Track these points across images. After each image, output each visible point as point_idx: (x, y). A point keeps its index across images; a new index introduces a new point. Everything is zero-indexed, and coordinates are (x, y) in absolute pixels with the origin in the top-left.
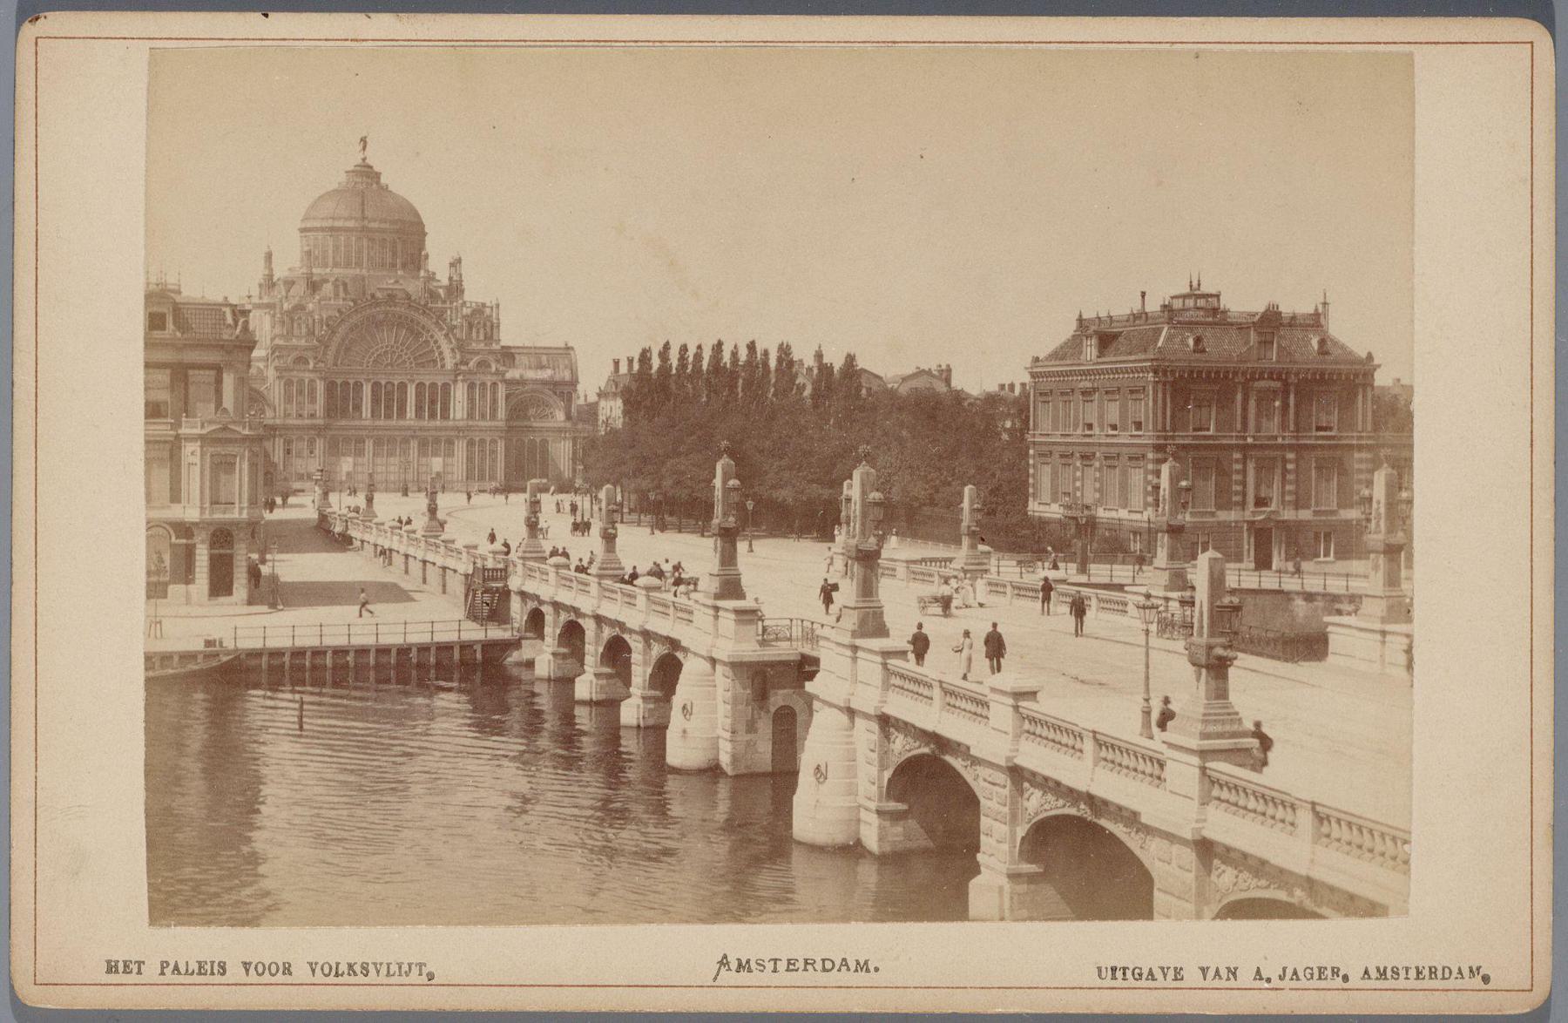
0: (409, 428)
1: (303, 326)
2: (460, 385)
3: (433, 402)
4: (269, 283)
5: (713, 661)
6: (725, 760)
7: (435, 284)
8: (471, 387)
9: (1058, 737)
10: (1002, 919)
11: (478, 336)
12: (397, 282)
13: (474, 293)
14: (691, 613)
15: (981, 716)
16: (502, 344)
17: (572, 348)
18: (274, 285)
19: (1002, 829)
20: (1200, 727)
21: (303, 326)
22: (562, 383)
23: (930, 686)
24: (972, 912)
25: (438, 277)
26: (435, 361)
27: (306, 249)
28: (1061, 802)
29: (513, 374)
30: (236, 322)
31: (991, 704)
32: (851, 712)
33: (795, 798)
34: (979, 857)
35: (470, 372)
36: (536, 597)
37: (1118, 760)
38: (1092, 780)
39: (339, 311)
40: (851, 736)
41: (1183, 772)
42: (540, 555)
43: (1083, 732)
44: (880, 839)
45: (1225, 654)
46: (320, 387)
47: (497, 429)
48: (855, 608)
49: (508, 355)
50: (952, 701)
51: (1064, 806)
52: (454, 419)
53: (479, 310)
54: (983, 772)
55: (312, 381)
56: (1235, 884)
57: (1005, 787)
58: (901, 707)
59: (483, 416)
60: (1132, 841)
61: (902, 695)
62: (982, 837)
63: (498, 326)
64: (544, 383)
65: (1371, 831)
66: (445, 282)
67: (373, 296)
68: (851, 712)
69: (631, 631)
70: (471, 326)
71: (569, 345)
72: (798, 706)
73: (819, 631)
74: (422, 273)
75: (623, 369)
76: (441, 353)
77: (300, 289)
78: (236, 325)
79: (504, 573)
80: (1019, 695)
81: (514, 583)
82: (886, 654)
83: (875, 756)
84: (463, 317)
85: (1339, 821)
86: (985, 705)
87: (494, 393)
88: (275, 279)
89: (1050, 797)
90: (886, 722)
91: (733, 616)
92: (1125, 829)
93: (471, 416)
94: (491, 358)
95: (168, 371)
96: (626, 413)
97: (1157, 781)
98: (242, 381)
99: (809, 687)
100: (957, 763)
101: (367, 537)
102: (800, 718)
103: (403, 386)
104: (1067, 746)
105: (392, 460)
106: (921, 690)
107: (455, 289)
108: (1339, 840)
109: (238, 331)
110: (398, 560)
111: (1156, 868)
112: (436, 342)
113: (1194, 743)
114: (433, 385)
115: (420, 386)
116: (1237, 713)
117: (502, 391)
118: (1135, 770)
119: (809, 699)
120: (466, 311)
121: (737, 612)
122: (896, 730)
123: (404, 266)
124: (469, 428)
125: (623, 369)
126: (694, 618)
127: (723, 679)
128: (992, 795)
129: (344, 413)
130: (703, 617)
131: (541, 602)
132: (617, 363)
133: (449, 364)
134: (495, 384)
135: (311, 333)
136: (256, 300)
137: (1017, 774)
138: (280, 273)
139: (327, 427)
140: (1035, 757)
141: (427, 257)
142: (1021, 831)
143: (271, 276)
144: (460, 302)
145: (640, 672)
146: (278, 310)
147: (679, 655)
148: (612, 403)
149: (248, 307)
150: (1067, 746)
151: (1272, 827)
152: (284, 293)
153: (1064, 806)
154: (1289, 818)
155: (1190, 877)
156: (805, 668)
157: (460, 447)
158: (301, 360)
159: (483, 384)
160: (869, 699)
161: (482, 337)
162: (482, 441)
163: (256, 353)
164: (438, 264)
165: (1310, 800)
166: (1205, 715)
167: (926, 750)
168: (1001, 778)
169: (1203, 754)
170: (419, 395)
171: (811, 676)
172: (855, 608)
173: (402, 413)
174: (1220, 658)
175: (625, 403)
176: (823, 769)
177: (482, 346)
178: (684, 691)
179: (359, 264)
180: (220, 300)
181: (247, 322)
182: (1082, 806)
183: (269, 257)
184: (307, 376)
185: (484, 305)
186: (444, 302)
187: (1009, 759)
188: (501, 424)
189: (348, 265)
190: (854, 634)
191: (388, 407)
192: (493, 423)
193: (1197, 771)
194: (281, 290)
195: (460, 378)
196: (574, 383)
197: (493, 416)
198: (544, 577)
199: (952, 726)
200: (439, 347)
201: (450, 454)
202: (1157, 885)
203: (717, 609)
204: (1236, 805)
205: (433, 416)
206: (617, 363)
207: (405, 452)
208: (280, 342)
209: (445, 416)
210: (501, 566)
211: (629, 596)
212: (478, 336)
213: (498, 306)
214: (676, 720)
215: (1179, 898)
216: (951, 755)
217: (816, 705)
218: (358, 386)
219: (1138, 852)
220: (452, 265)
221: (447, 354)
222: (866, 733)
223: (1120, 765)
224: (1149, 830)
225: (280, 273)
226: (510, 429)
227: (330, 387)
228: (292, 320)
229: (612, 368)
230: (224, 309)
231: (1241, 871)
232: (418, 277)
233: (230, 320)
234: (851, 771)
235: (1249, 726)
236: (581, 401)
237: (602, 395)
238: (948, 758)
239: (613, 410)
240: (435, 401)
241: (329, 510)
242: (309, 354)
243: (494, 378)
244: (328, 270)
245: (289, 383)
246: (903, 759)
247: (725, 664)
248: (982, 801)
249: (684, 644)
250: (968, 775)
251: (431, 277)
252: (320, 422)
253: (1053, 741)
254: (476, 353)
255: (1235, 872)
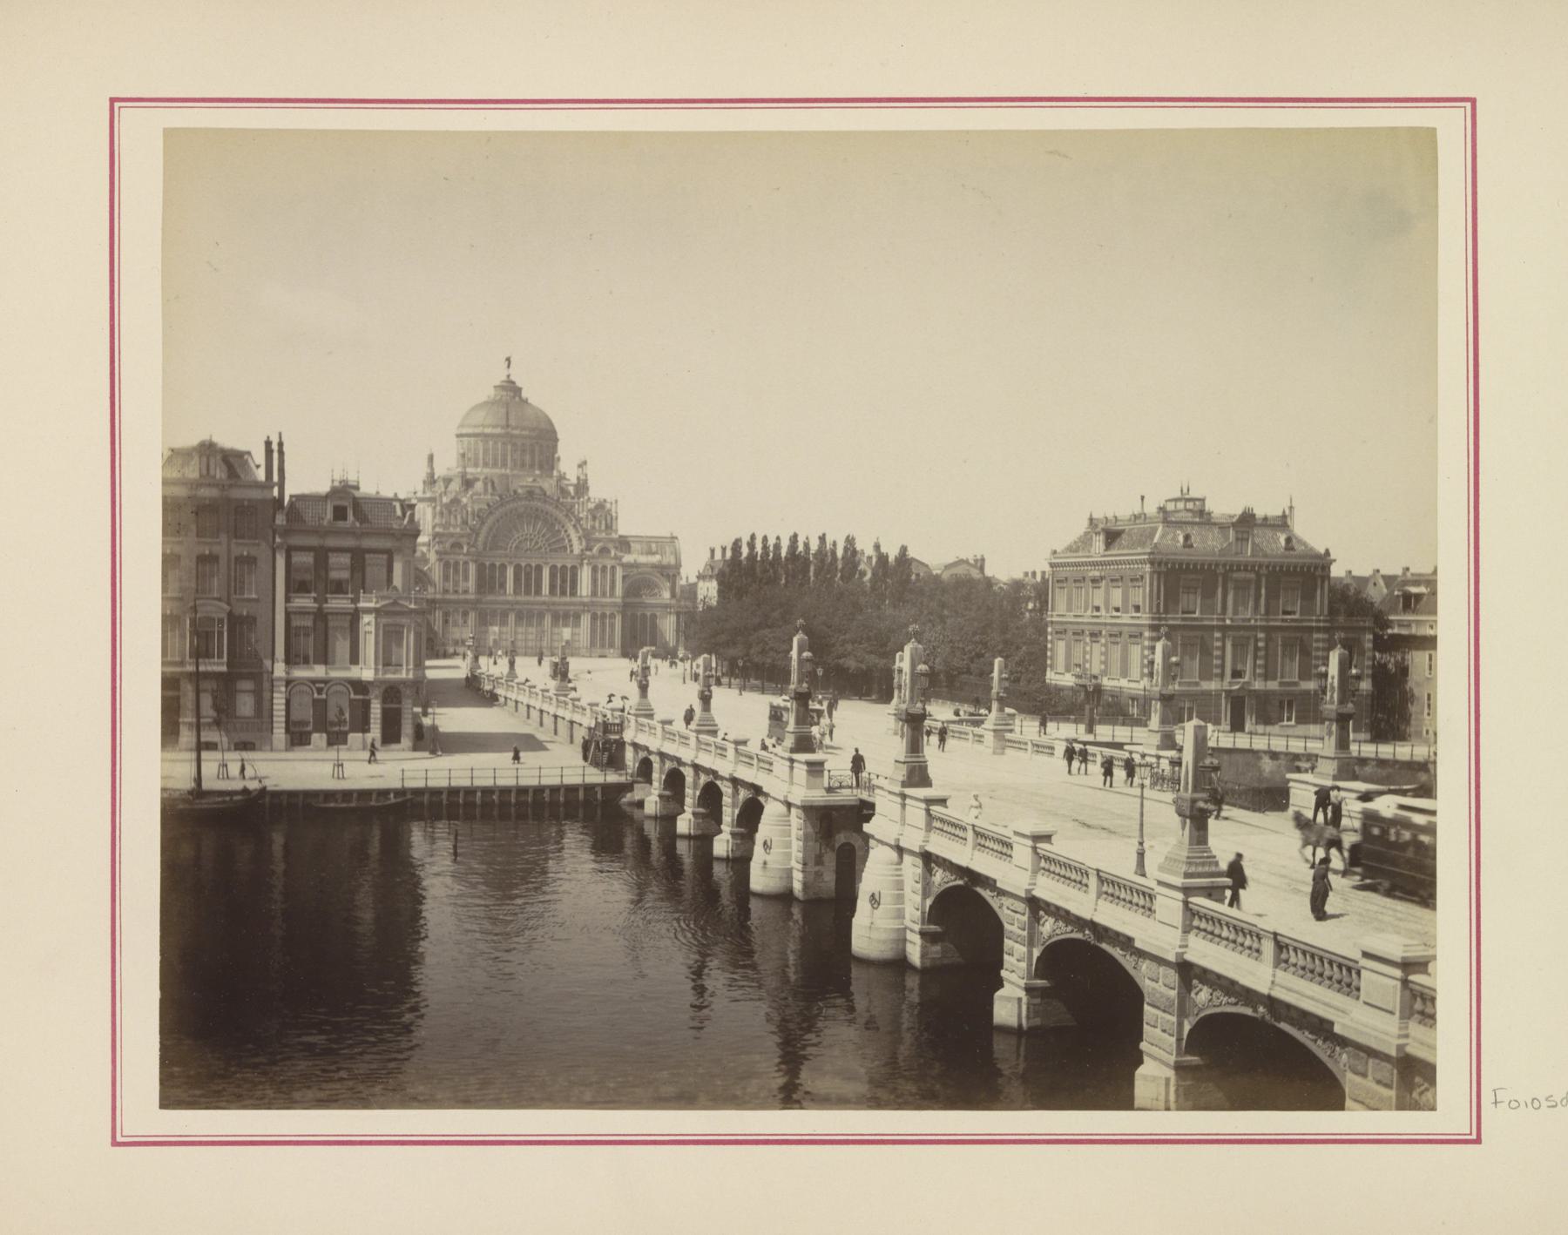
0: (544, 603)
1: (459, 517)
2: (585, 567)
3: (564, 581)
4: (431, 481)
5: (789, 805)
6: (797, 886)
7: (566, 482)
8: (594, 570)
9: (1068, 874)
10: (1168, 1109)
11: (600, 527)
12: (534, 480)
13: (596, 493)
14: (771, 764)
15: (1006, 854)
16: (622, 531)
17: (676, 538)
18: (435, 482)
19: (1021, 950)
20: (1184, 868)
21: (459, 517)
22: (668, 567)
23: (965, 829)
24: (1137, 1103)
25: (568, 477)
26: (565, 548)
27: (461, 451)
28: (1069, 928)
29: (628, 558)
30: (404, 515)
31: (1015, 846)
32: (900, 850)
33: (854, 920)
34: (1144, 1046)
35: (593, 557)
36: (646, 749)
37: (1217, 931)
38: (1096, 910)
39: (488, 505)
40: (900, 869)
41: (1170, 906)
42: (648, 712)
43: (1090, 871)
44: (923, 956)
45: (1206, 807)
46: (472, 568)
47: (615, 605)
48: (904, 763)
49: (624, 544)
50: (983, 842)
51: (1072, 931)
52: (581, 596)
53: (601, 506)
54: (1007, 901)
55: (466, 563)
56: (1210, 1000)
57: (1024, 914)
58: (941, 846)
59: (604, 595)
60: (1127, 962)
61: (1053, 879)
62: (1006, 957)
63: (617, 518)
64: (654, 566)
65: (1321, 959)
66: (574, 481)
67: (515, 492)
68: (900, 850)
69: (722, 778)
70: (594, 518)
71: (674, 535)
72: (857, 842)
73: (875, 782)
74: (555, 473)
75: (718, 556)
76: (570, 541)
77: (455, 486)
78: (404, 515)
79: (621, 727)
80: (1037, 838)
81: (628, 736)
82: (929, 802)
83: (919, 886)
84: (589, 511)
85: (1295, 949)
86: (1009, 845)
87: (613, 575)
88: (436, 477)
89: (1061, 924)
90: (928, 859)
91: (805, 767)
92: (1310, 1036)
93: (594, 593)
94: (610, 546)
95: (349, 555)
96: (720, 592)
97: (1148, 913)
98: (407, 564)
99: (867, 828)
100: (986, 894)
101: (509, 695)
102: (859, 853)
103: (539, 569)
104: (1075, 881)
105: (530, 630)
106: (957, 832)
107: (582, 487)
108: (1295, 965)
109: (406, 521)
110: (535, 714)
111: (1147, 985)
112: (566, 531)
113: (1178, 881)
114: (564, 567)
115: (553, 568)
116: (1215, 857)
117: (619, 573)
118: (1131, 902)
119: (867, 837)
120: (591, 506)
121: (809, 764)
122: (1046, 913)
123: (541, 467)
124: (593, 604)
125: (718, 556)
126: (774, 768)
127: (796, 820)
128: (1013, 919)
129: (492, 590)
130: (781, 767)
131: (650, 753)
132: (713, 551)
133: (577, 551)
134: (613, 568)
135: (465, 522)
136: (420, 494)
137: (1036, 906)
138: (440, 472)
139: (478, 601)
140: (1049, 890)
141: (559, 459)
142: (1036, 953)
143: (432, 475)
144: (586, 498)
145: (729, 814)
146: (438, 503)
147: (761, 799)
148: (708, 584)
149: (414, 501)
150: (1075, 881)
151: (1241, 953)
152: (443, 489)
153: (1072, 931)
154: (1255, 945)
155: (1173, 994)
156: (864, 811)
157: (586, 620)
158: (457, 545)
159: (604, 568)
160: (914, 839)
161: (603, 527)
162: (604, 616)
163: (422, 539)
164: (567, 466)
165: (1271, 930)
166: (1188, 858)
167: (960, 882)
168: (1021, 906)
169: (1187, 891)
170: (553, 576)
171: (868, 818)
172: (904, 763)
173: (538, 592)
174: (1202, 811)
175: (719, 584)
176: (877, 897)
177: (603, 535)
178: (764, 830)
179: (504, 465)
180: (391, 495)
181: (412, 515)
182: (1087, 932)
183: (431, 458)
184: (461, 558)
185: (605, 501)
186: (573, 498)
187: (1028, 891)
188: (619, 600)
189: (495, 465)
190: (904, 784)
191: (528, 586)
192: (613, 600)
193: (1181, 904)
194: (440, 487)
195: (585, 561)
196: (678, 566)
197: (612, 595)
198: (653, 731)
199: (983, 863)
200: (568, 536)
201: (577, 624)
202: (1147, 999)
203: (792, 761)
204: (1212, 933)
205: (563, 593)
206: (713, 551)
207: (540, 623)
208: (438, 529)
209: (573, 593)
210: (617, 721)
211: (721, 748)
212: (600, 527)
213: (616, 502)
214: (758, 849)
215: (1164, 1011)
216: (981, 887)
217: (872, 842)
218: (503, 567)
219: (1132, 972)
220: (580, 466)
221: (575, 542)
222: (912, 869)
223: (1118, 898)
224: (1141, 954)
225: (440, 472)
226: (625, 605)
227: (481, 568)
228: (450, 512)
229: (709, 555)
230: (394, 503)
231: (1214, 990)
232: (551, 476)
233: (399, 512)
234: (900, 899)
235: (1224, 866)
236: (683, 582)
237: (701, 577)
238: (979, 890)
239: (709, 591)
240: (565, 580)
241: (479, 671)
242: (464, 540)
243: (613, 562)
244: (479, 470)
245: (447, 565)
246: (942, 889)
247: (798, 807)
248: (1007, 926)
249: (765, 790)
250: (994, 903)
251: (562, 477)
252: (471, 597)
253: (1064, 877)
254: (599, 540)
255: (1210, 991)
